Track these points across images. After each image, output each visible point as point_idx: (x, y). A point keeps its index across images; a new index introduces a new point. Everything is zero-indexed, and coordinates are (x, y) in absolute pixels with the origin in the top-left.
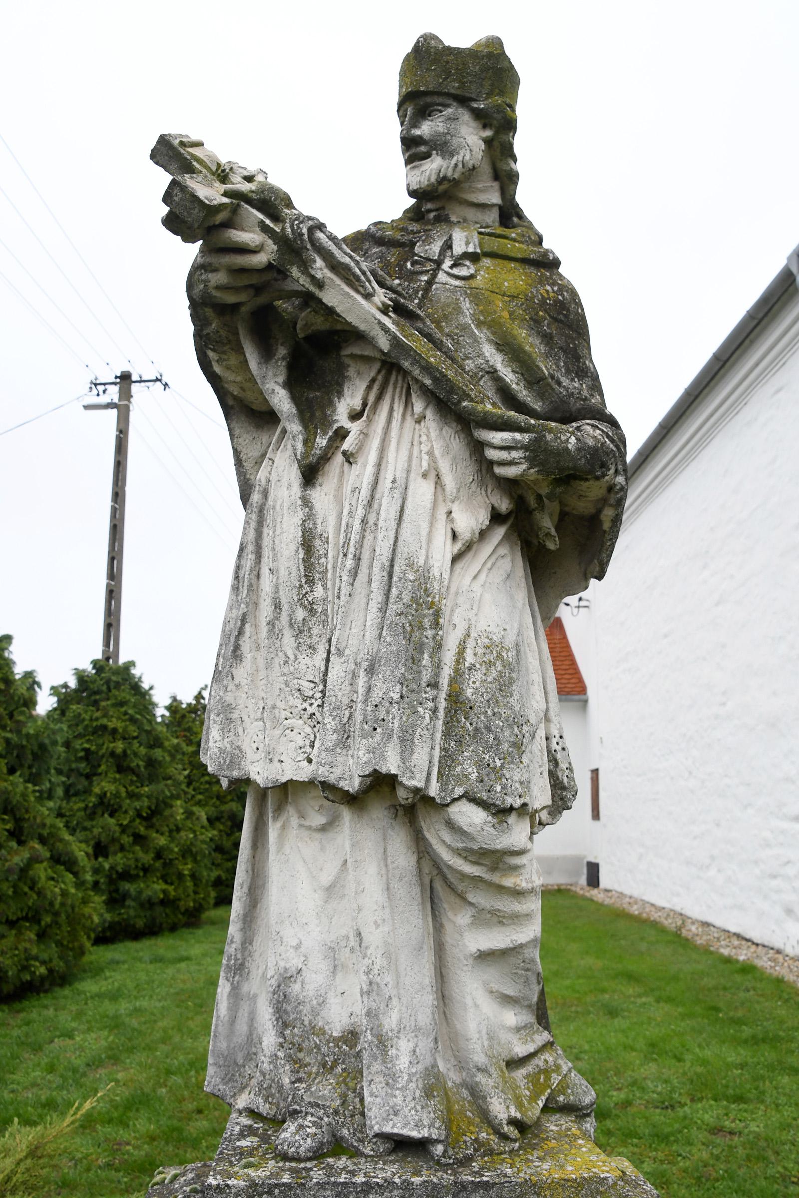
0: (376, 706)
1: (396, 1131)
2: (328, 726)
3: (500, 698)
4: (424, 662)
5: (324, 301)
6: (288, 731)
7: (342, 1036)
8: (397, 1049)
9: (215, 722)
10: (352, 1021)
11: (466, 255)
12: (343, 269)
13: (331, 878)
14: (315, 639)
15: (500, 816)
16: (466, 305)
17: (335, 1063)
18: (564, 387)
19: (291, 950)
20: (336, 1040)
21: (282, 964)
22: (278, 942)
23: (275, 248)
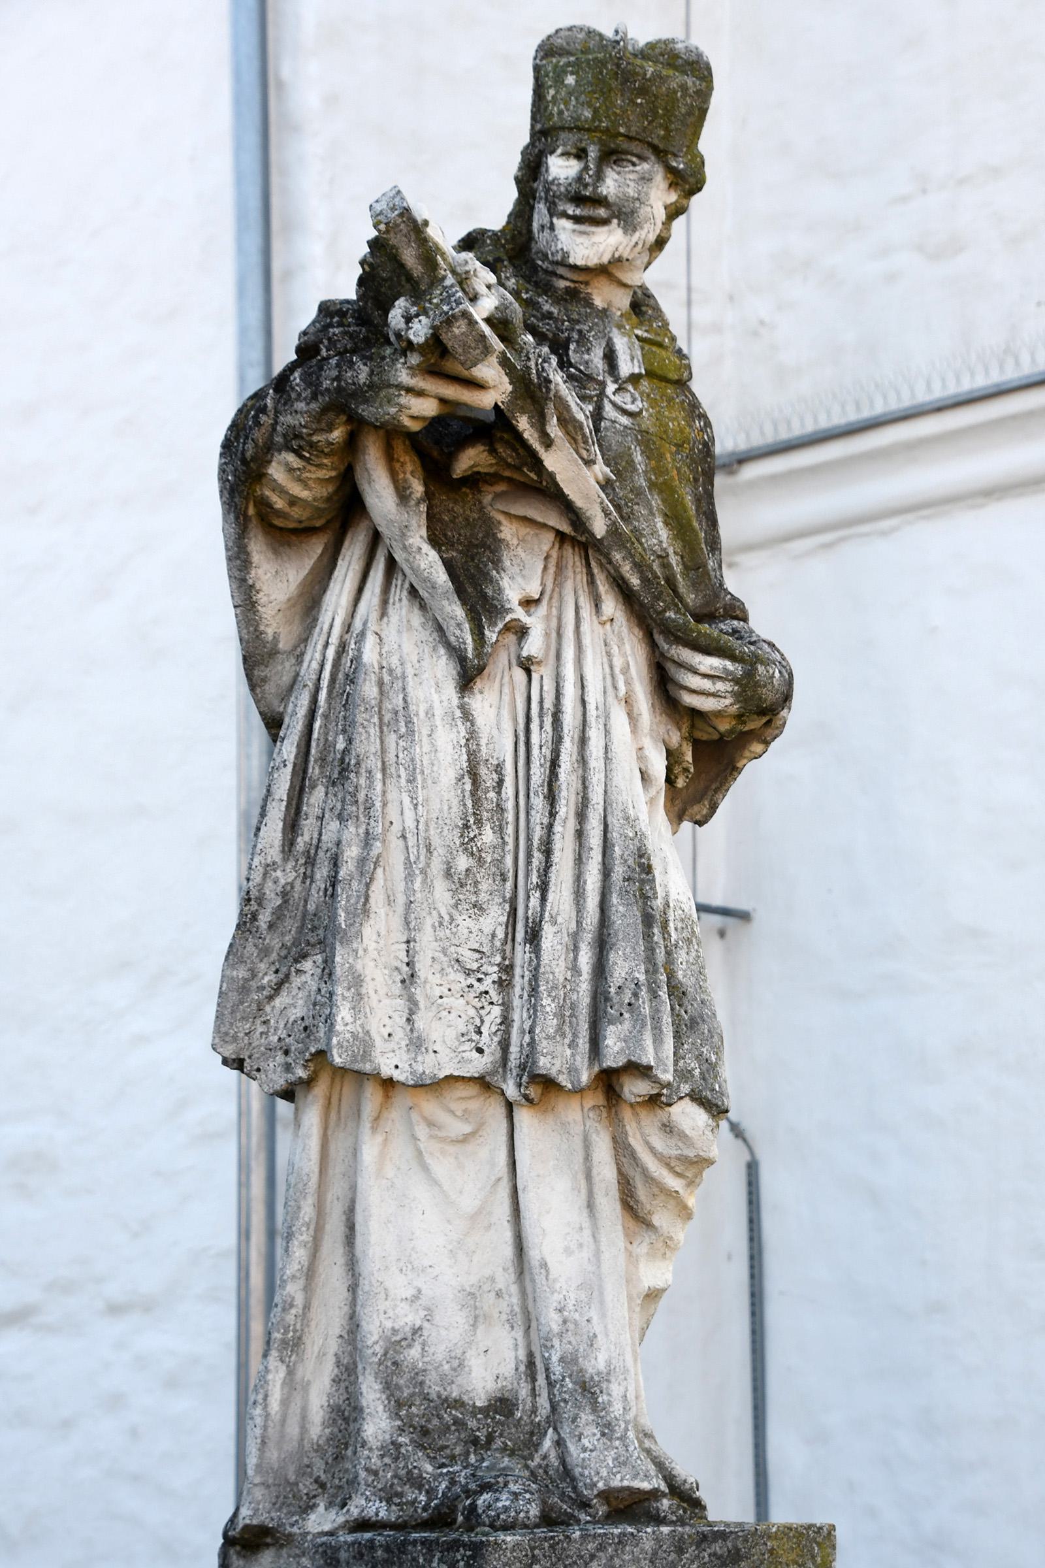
0: (619, 988)
1: (626, 1483)
2: (548, 1009)
4: (656, 938)
5: (546, 463)
6: (445, 1013)
7: (489, 1406)
8: (609, 1395)
9: (344, 998)
10: (499, 1385)
12: (575, 427)
13: (477, 1203)
14: (483, 897)
17: (490, 1438)
19: (403, 1304)
20: (481, 1410)
21: (389, 1324)
22: (382, 1295)
23: (510, 388)
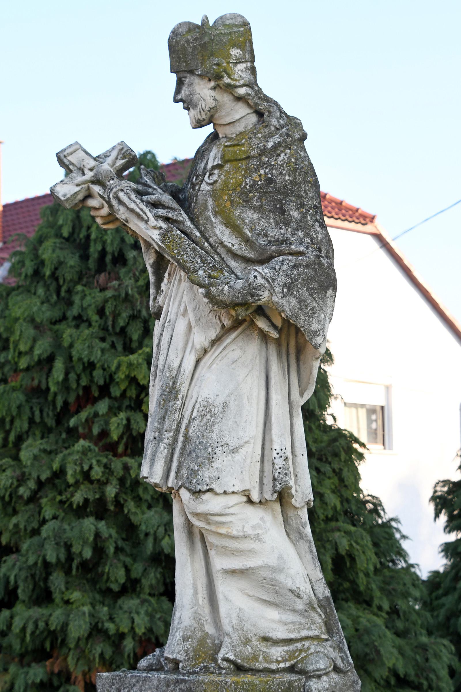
3: (205, 434)
11: (214, 168)
15: (197, 495)
16: (210, 203)
18: (271, 236)
